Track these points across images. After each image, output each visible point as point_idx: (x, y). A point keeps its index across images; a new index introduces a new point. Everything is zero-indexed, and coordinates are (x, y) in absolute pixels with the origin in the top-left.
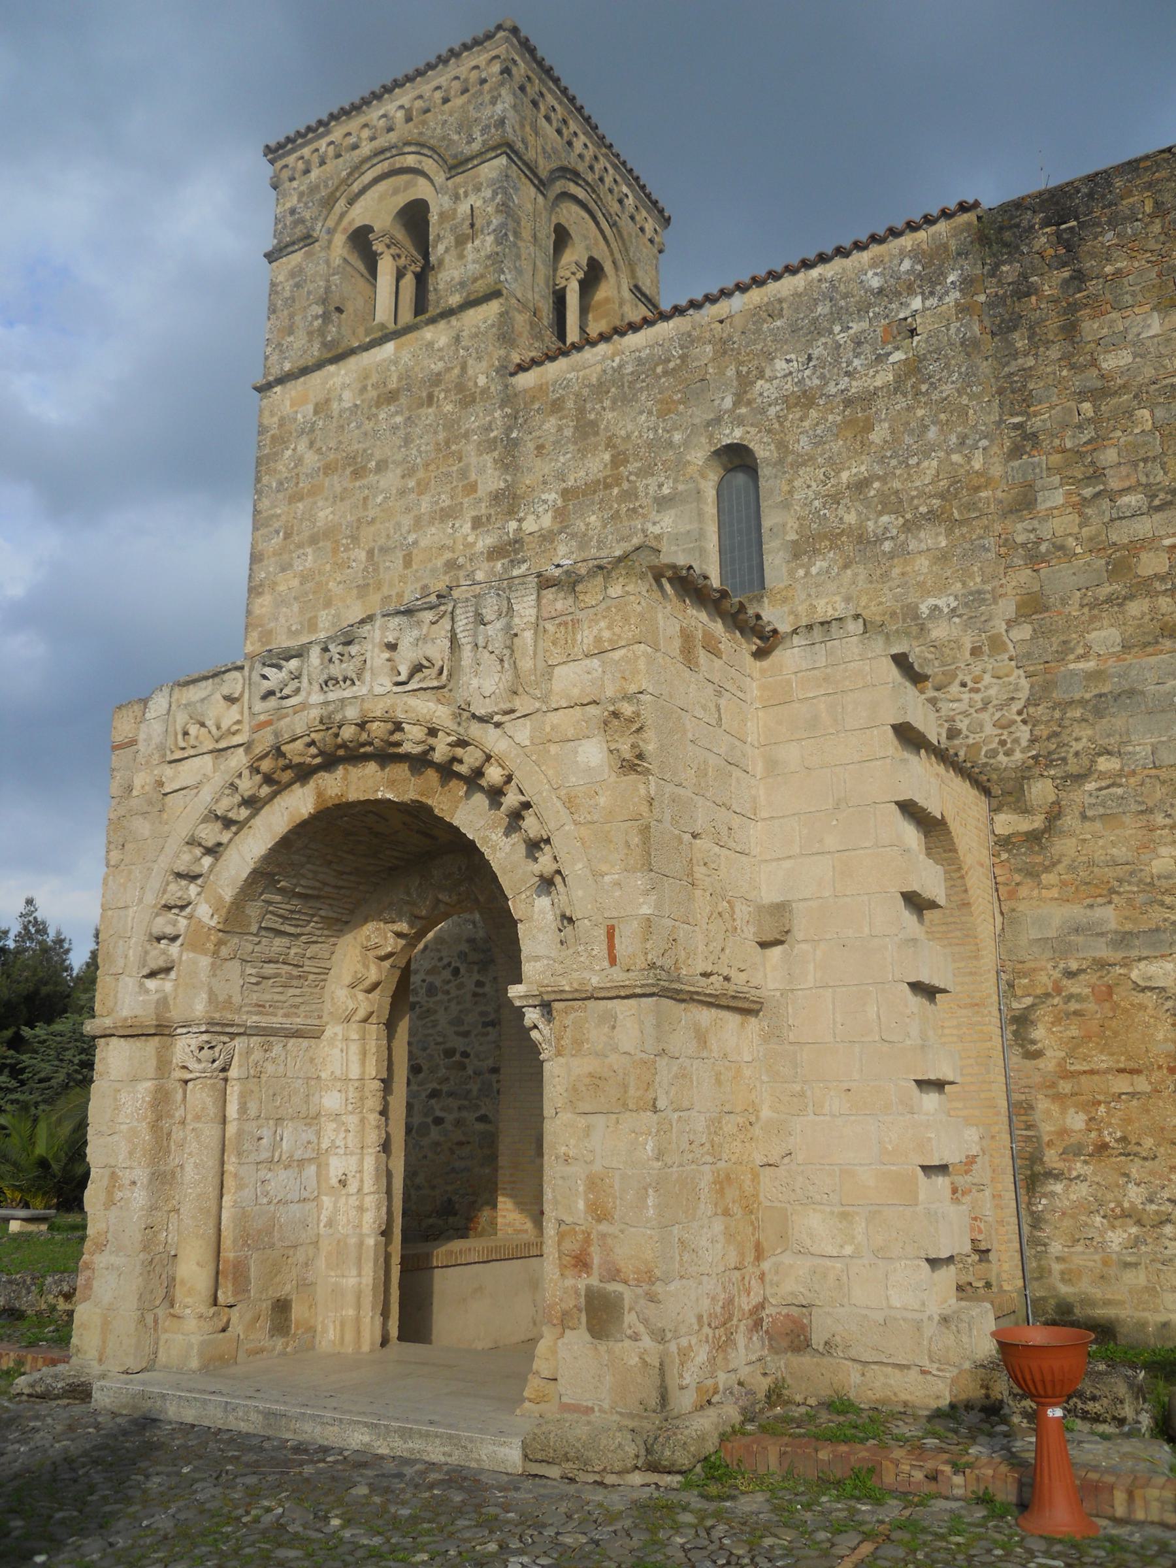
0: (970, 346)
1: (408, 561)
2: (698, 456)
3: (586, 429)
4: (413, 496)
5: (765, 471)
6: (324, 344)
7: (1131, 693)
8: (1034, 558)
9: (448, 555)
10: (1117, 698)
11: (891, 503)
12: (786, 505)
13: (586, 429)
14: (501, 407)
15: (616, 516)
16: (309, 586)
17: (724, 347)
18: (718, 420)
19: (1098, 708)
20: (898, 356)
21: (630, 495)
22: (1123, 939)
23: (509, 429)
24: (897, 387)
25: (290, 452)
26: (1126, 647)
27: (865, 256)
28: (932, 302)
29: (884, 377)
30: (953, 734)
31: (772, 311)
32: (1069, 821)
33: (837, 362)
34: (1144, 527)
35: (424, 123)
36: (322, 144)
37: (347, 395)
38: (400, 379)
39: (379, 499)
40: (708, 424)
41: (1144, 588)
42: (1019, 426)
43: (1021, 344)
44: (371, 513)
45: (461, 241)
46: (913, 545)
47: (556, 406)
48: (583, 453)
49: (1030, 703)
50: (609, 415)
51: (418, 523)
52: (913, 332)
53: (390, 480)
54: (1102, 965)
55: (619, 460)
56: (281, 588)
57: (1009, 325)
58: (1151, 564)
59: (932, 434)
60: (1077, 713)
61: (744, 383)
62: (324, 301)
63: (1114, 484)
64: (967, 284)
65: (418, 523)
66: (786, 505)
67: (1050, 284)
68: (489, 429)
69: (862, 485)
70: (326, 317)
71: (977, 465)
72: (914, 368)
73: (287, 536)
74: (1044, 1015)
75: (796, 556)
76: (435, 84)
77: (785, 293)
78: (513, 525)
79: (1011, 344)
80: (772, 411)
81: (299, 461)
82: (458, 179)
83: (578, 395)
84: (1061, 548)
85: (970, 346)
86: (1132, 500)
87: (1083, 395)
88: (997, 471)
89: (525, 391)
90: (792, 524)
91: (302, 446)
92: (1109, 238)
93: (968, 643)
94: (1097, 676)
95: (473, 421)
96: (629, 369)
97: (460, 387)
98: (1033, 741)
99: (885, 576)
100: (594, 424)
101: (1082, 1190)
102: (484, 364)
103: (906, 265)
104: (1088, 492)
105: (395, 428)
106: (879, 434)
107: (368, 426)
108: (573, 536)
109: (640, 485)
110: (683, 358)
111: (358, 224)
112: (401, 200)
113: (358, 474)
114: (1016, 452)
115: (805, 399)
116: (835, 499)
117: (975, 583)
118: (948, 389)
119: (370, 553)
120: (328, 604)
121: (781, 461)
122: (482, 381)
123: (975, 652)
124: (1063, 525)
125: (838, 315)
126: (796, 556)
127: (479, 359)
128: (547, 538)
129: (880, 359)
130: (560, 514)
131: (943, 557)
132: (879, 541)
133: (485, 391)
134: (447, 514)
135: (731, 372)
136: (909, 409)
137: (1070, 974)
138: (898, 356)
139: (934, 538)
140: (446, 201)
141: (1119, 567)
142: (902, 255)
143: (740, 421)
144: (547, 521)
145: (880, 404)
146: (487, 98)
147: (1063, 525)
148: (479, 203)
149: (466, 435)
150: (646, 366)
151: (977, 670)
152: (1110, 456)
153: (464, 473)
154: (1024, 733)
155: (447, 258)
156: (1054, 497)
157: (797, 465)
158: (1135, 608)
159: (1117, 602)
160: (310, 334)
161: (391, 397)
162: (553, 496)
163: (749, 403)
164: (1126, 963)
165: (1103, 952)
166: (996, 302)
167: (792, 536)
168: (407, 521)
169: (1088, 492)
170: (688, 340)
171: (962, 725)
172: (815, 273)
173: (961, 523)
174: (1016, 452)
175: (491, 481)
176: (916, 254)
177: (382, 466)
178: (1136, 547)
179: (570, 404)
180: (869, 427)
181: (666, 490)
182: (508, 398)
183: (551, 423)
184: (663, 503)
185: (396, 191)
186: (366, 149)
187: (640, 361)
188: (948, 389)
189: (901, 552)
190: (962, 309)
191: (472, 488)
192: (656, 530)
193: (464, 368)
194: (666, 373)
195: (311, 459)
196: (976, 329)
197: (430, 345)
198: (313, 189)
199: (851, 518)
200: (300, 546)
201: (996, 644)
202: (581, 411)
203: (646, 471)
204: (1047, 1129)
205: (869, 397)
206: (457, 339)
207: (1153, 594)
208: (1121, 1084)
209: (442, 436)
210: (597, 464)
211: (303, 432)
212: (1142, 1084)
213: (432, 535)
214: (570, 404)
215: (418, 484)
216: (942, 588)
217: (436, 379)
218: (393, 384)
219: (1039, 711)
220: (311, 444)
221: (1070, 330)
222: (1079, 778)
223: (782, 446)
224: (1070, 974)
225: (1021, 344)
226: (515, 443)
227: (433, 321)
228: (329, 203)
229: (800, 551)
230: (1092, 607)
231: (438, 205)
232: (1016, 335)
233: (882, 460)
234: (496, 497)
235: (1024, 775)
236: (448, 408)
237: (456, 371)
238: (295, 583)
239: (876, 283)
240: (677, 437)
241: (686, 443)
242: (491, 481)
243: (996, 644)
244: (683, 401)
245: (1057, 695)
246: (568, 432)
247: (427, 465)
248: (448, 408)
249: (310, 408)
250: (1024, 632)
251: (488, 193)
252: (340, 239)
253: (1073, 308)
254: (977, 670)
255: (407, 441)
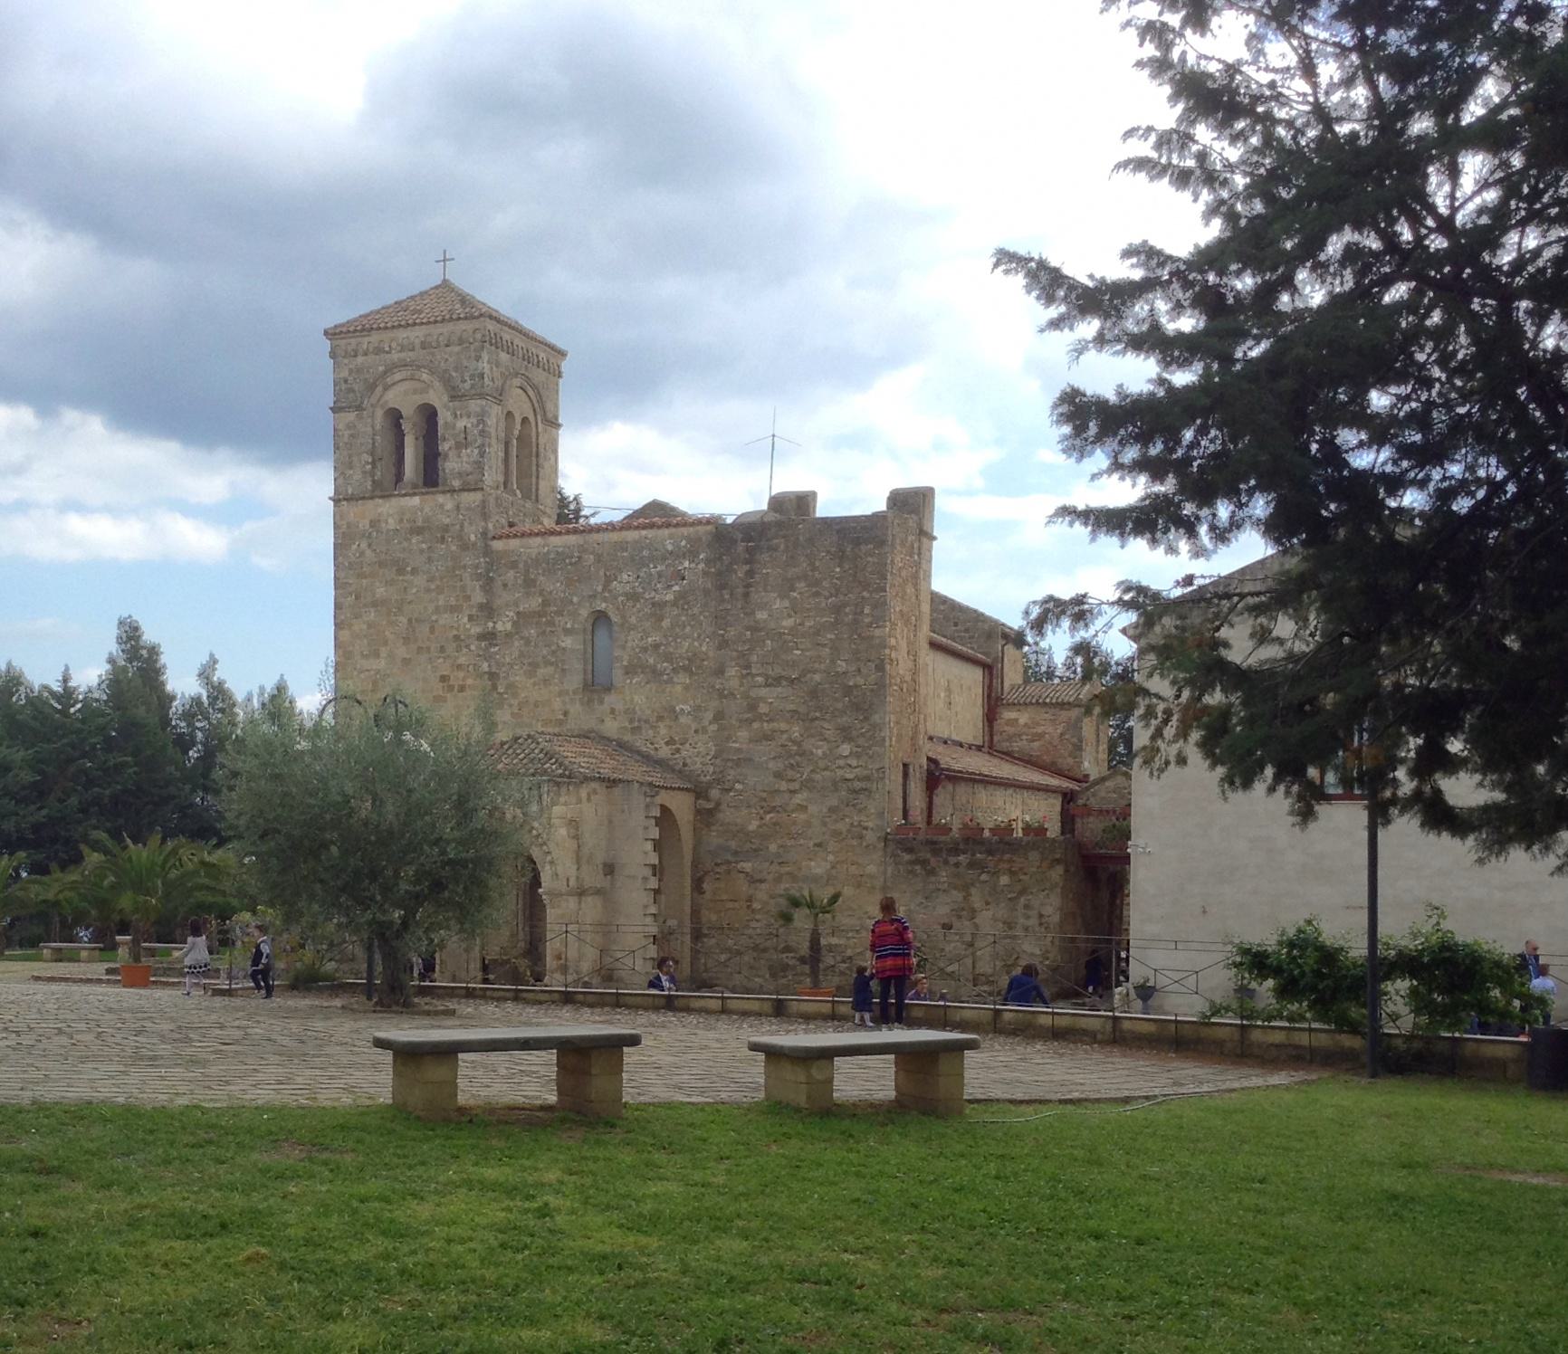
0: (706, 592)
1: (432, 630)
2: (584, 613)
3: (529, 583)
4: (434, 594)
5: (616, 628)
6: (374, 481)
7: (750, 760)
8: (721, 695)
9: (455, 632)
10: (745, 760)
11: (668, 658)
12: (624, 647)
13: (529, 583)
14: (484, 557)
15: (544, 632)
16: (372, 631)
17: (599, 558)
18: (593, 597)
19: (738, 763)
20: (676, 588)
21: (551, 623)
22: (736, 853)
23: (488, 571)
24: (674, 604)
25: (355, 547)
26: (751, 741)
27: (666, 532)
28: (693, 565)
29: (670, 597)
30: (685, 765)
31: (622, 546)
32: (723, 807)
33: (649, 583)
34: (763, 692)
35: (433, 354)
36: (366, 340)
37: (391, 521)
38: (424, 522)
39: (414, 590)
40: (590, 596)
41: (760, 718)
42: (723, 636)
43: (727, 597)
44: (410, 598)
45: (459, 446)
46: (675, 680)
47: (514, 565)
48: (527, 594)
49: (715, 757)
50: (542, 578)
51: (437, 610)
52: (683, 579)
53: (420, 581)
54: (729, 862)
55: (545, 603)
56: (356, 628)
57: (722, 587)
58: (763, 709)
59: (688, 629)
60: (730, 764)
61: (608, 581)
62: (372, 454)
63: (754, 671)
64: (708, 562)
65: (437, 610)
66: (624, 647)
67: (741, 571)
68: (477, 567)
69: (656, 646)
70: (373, 463)
71: (704, 649)
72: (682, 596)
73: (356, 598)
74: (707, 879)
75: (627, 673)
76: (440, 330)
77: (629, 539)
78: (491, 625)
79: (722, 595)
80: (621, 598)
81: (362, 554)
82: (456, 403)
83: (526, 562)
84: (733, 694)
85: (706, 592)
86: (760, 679)
87: (748, 628)
88: (711, 654)
89: (498, 552)
90: (626, 657)
91: (364, 545)
92: (765, 557)
93: (694, 727)
94: (739, 750)
95: (468, 560)
96: (552, 556)
97: (460, 538)
98: (714, 773)
99: (663, 691)
100: (534, 581)
101: (713, 941)
102: (473, 528)
103: (683, 543)
104: (744, 672)
105: (422, 551)
106: (666, 623)
107: (405, 544)
108: (522, 638)
109: (557, 619)
110: (579, 558)
111: (391, 405)
112: (419, 400)
113: (401, 571)
114: (720, 648)
115: (634, 597)
116: (645, 650)
117: (698, 701)
118: (696, 611)
119: (410, 620)
120: (386, 643)
121: (622, 625)
122: (473, 538)
123: (696, 731)
124: (734, 683)
125: (652, 559)
126: (627, 673)
127: (471, 524)
128: (508, 635)
129: (670, 587)
130: (515, 624)
131: (687, 688)
132: (661, 674)
133: (474, 544)
134: (454, 609)
135: (602, 573)
136: (679, 615)
137: (717, 864)
138: (676, 588)
139: (683, 678)
140: (450, 418)
141: (752, 707)
142: (683, 537)
143: (605, 600)
144: (509, 626)
145: (668, 609)
146: (473, 355)
147: (734, 683)
148: (469, 425)
149: (465, 567)
150: (561, 556)
151: (696, 739)
152: (754, 658)
153: (463, 588)
154: (711, 769)
155: (451, 454)
156: (732, 671)
157: (630, 629)
158: (756, 725)
159: (750, 722)
160: (364, 473)
161: (418, 531)
162: (511, 614)
163: (610, 591)
164: (736, 862)
165: (730, 858)
166: (719, 573)
167: (625, 663)
168: (431, 608)
169: (744, 672)
170: (582, 549)
171: (688, 761)
172: (644, 533)
173: (697, 674)
174: (720, 648)
175: (479, 597)
176: (689, 539)
177: (414, 571)
178: (762, 699)
179: (521, 566)
180: (661, 619)
181: (569, 626)
182: (487, 551)
183: (511, 574)
184: (567, 632)
185: (415, 392)
186: (395, 356)
187: (558, 553)
188: (696, 611)
189: (670, 681)
190: (705, 573)
191: (468, 598)
192: (563, 645)
193: (462, 526)
194: (571, 564)
195: (368, 552)
196: (709, 585)
197: (442, 506)
198: (359, 371)
199: (651, 661)
200: (365, 605)
201: (705, 730)
202: (527, 571)
203: (559, 613)
204: (704, 920)
205: (662, 605)
206: (458, 508)
207: (762, 720)
208: (730, 905)
209: (450, 564)
210: (534, 603)
211: (363, 535)
212: (736, 905)
213: (445, 619)
214: (521, 566)
215: (438, 587)
216: (685, 702)
217: (446, 528)
218: (420, 523)
219: (718, 761)
220: (370, 545)
221: (746, 595)
222: (728, 790)
223: (623, 617)
224: (717, 864)
225: (727, 597)
226: (492, 580)
227: (444, 492)
228: (371, 387)
229: (629, 671)
230: (741, 721)
231: (444, 417)
232: (724, 592)
233: (665, 636)
234: (481, 607)
235: (709, 785)
236: (454, 548)
237: (458, 527)
238: (365, 627)
239: (670, 548)
240: (575, 599)
241: (579, 603)
242: (479, 597)
243: (705, 730)
244: (579, 581)
245: (725, 756)
246: (519, 581)
247: (441, 579)
248: (454, 548)
249: (367, 522)
250: (714, 727)
251: (474, 420)
252: (379, 413)
253: (748, 586)
254: (696, 739)
255: (430, 560)
